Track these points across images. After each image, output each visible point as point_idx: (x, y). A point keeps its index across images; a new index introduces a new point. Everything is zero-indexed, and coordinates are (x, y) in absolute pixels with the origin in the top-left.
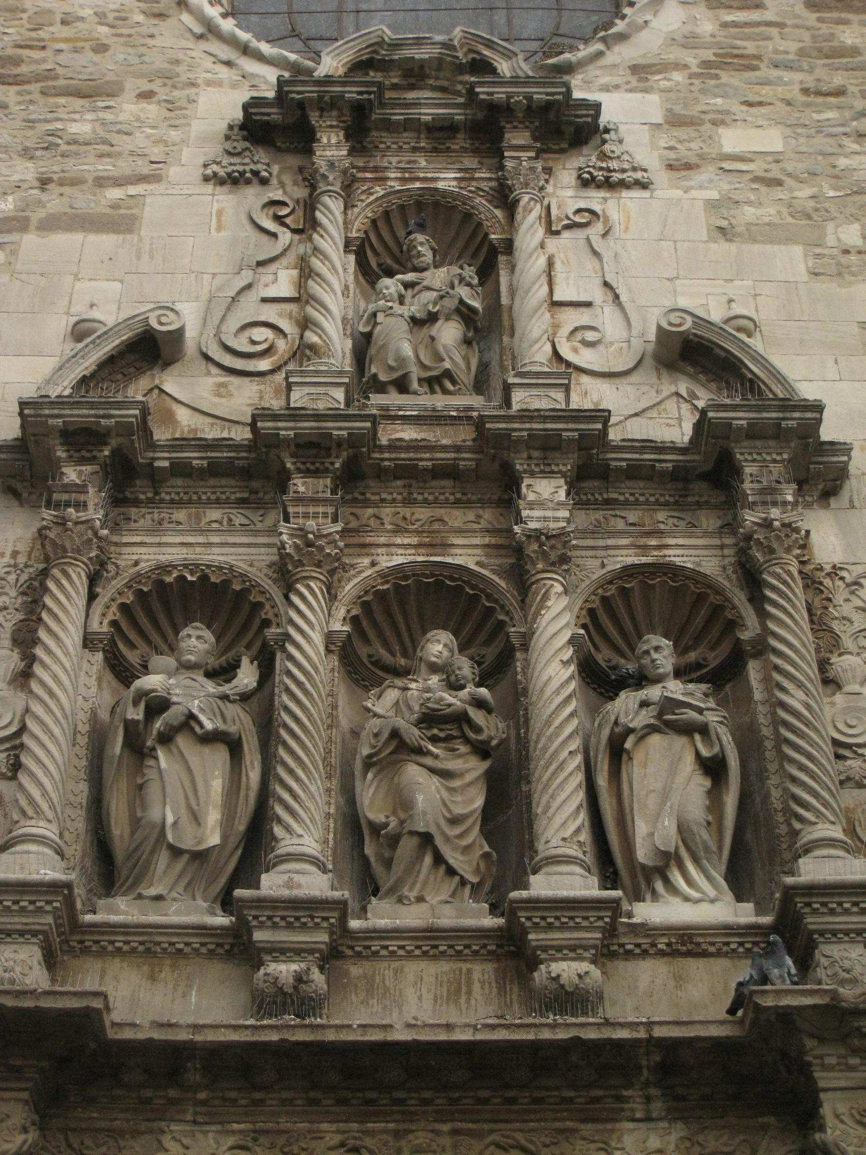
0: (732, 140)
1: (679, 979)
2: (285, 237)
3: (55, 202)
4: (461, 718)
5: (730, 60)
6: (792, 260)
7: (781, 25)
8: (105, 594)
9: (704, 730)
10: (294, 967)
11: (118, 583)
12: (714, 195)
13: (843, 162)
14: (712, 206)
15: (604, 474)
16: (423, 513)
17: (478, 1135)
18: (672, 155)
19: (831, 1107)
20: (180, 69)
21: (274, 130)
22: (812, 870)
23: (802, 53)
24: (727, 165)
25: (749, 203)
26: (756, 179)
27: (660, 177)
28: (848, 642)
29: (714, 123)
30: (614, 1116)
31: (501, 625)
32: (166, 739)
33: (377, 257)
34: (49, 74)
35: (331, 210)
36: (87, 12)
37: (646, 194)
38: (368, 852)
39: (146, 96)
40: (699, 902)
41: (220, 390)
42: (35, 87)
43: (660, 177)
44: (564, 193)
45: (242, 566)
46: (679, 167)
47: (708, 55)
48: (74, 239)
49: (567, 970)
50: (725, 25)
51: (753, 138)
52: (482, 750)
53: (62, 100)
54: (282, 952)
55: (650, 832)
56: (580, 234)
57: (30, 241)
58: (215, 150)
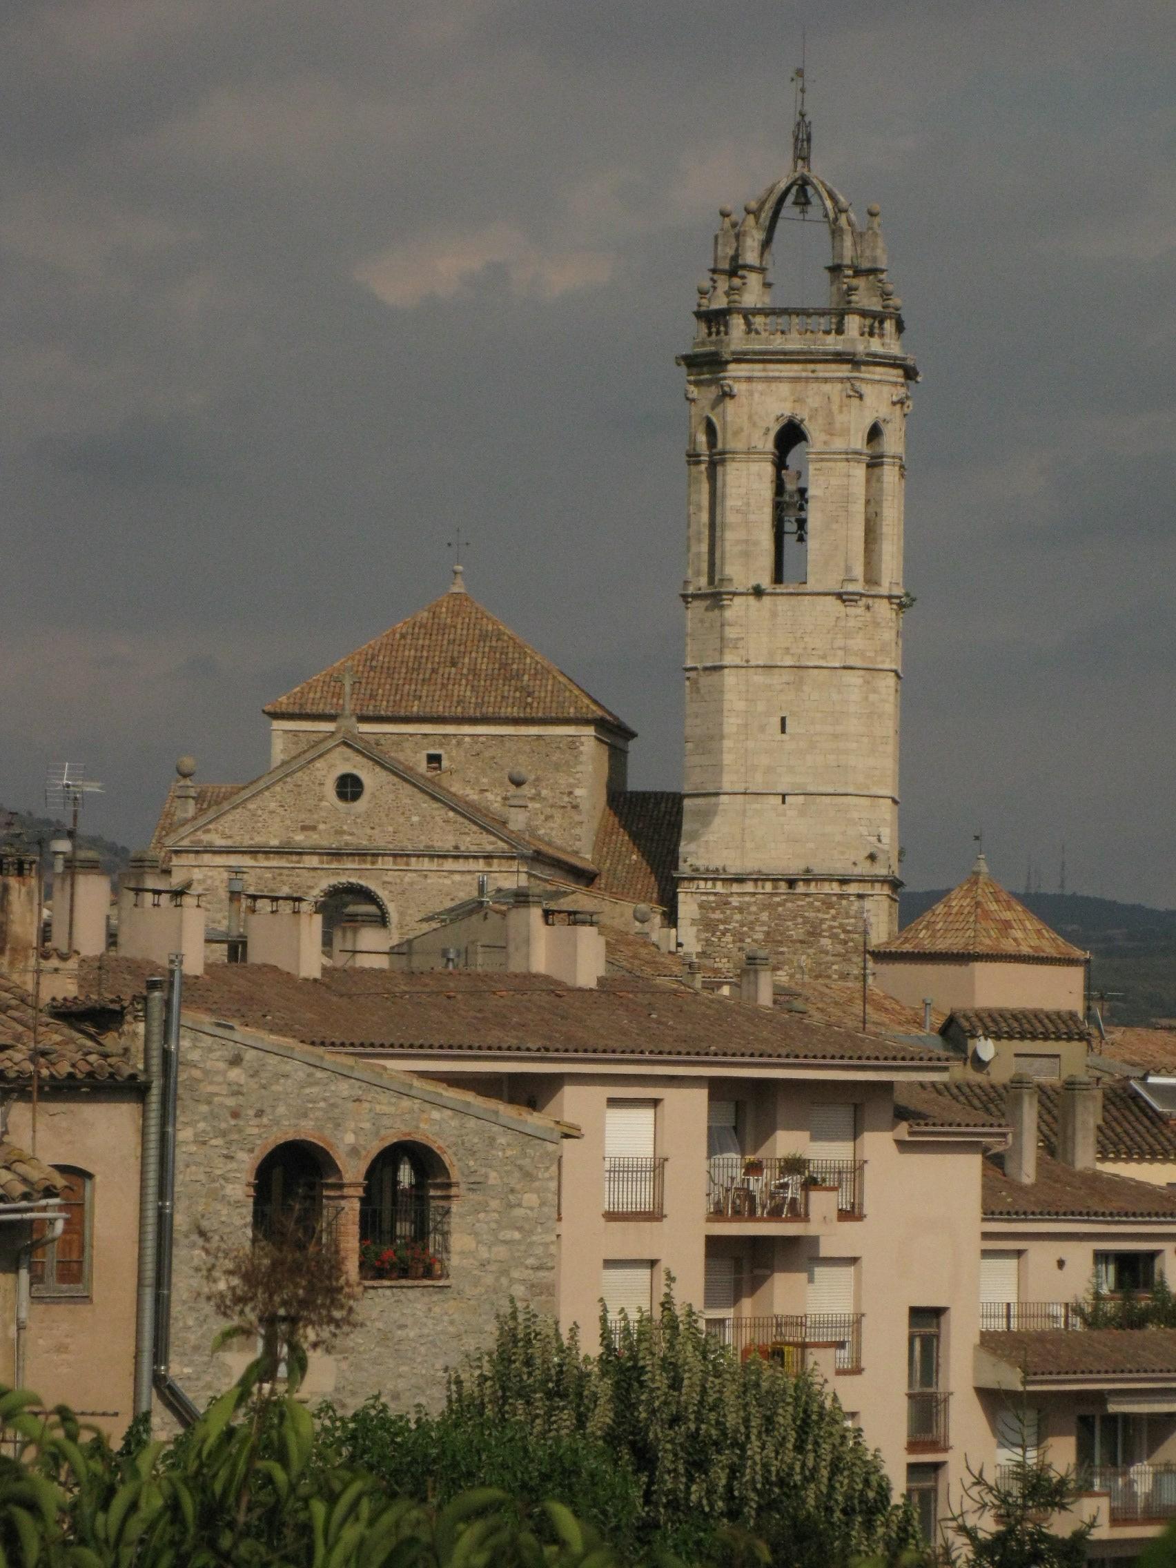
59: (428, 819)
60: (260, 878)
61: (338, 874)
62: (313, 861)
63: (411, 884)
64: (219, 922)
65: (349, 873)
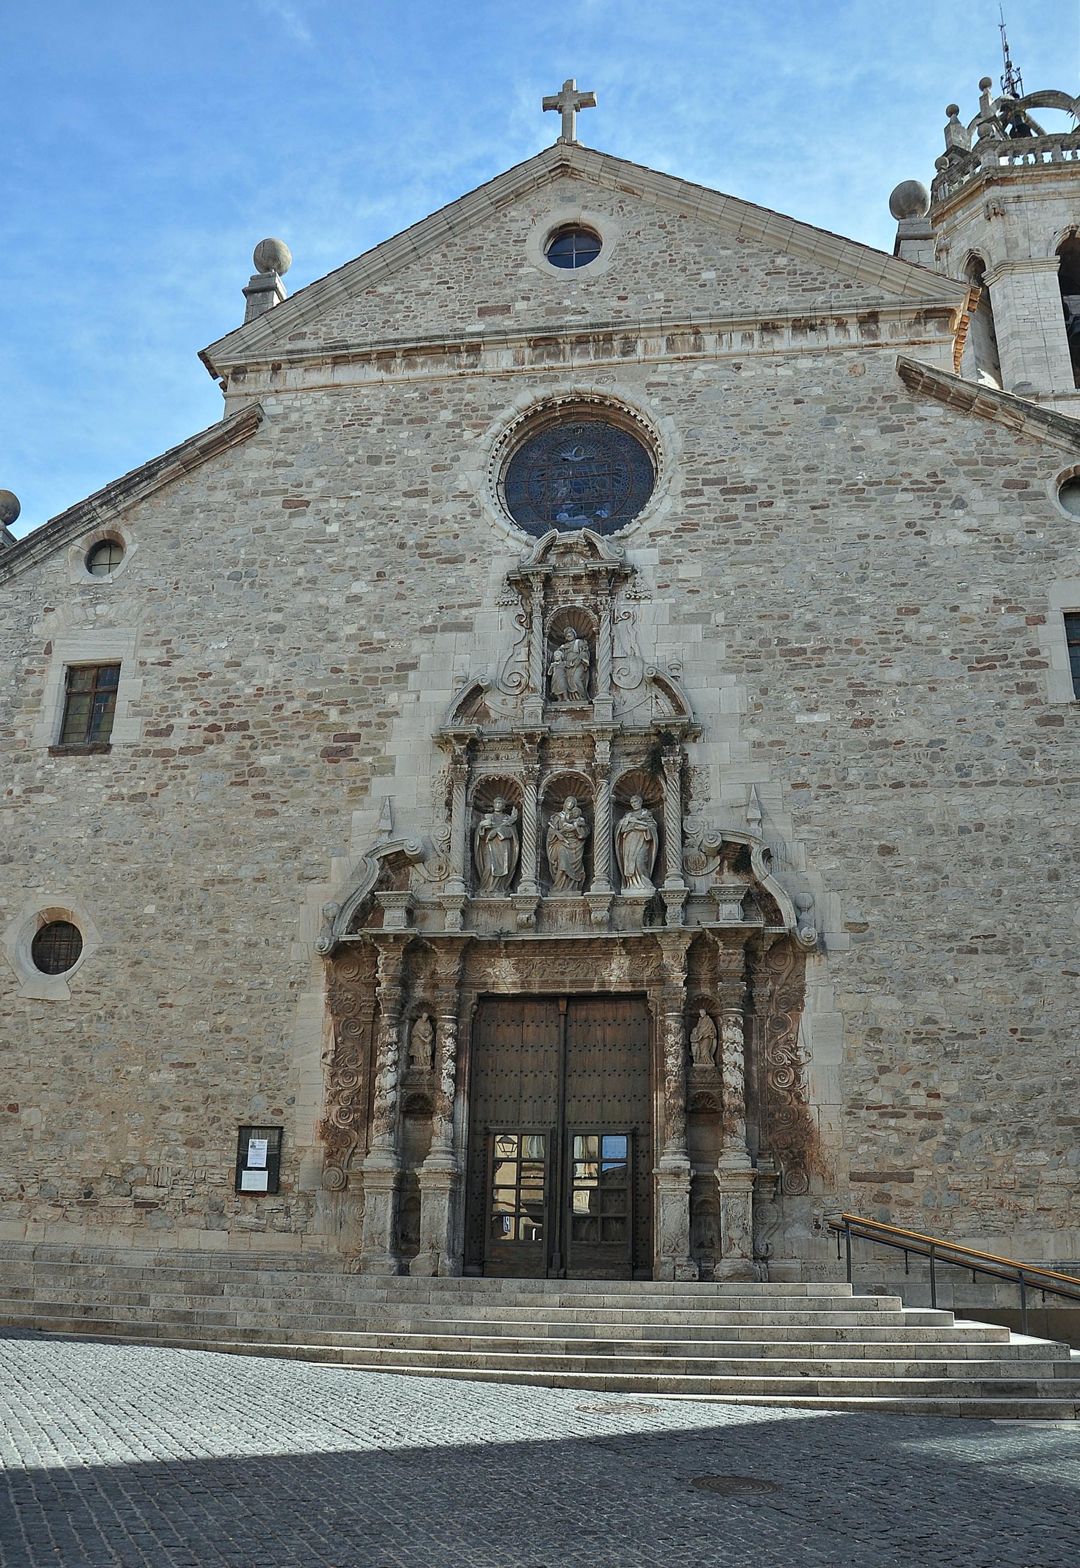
0: (683, 571)
6: (696, 631)
7: (709, 505)
11: (475, 783)
12: (673, 601)
13: (723, 580)
14: (672, 606)
18: (660, 580)
20: (485, 546)
21: (519, 582)
24: (679, 584)
25: (686, 603)
27: (655, 592)
33: (555, 639)
37: (649, 602)
39: (475, 561)
45: (512, 776)
47: (679, 524)
51: (690, 570)
53: (444, 566)
55: (629, 868)
57: (438, 635)
58: (498, 589)
59: (736, 272)
64: (310, 484)
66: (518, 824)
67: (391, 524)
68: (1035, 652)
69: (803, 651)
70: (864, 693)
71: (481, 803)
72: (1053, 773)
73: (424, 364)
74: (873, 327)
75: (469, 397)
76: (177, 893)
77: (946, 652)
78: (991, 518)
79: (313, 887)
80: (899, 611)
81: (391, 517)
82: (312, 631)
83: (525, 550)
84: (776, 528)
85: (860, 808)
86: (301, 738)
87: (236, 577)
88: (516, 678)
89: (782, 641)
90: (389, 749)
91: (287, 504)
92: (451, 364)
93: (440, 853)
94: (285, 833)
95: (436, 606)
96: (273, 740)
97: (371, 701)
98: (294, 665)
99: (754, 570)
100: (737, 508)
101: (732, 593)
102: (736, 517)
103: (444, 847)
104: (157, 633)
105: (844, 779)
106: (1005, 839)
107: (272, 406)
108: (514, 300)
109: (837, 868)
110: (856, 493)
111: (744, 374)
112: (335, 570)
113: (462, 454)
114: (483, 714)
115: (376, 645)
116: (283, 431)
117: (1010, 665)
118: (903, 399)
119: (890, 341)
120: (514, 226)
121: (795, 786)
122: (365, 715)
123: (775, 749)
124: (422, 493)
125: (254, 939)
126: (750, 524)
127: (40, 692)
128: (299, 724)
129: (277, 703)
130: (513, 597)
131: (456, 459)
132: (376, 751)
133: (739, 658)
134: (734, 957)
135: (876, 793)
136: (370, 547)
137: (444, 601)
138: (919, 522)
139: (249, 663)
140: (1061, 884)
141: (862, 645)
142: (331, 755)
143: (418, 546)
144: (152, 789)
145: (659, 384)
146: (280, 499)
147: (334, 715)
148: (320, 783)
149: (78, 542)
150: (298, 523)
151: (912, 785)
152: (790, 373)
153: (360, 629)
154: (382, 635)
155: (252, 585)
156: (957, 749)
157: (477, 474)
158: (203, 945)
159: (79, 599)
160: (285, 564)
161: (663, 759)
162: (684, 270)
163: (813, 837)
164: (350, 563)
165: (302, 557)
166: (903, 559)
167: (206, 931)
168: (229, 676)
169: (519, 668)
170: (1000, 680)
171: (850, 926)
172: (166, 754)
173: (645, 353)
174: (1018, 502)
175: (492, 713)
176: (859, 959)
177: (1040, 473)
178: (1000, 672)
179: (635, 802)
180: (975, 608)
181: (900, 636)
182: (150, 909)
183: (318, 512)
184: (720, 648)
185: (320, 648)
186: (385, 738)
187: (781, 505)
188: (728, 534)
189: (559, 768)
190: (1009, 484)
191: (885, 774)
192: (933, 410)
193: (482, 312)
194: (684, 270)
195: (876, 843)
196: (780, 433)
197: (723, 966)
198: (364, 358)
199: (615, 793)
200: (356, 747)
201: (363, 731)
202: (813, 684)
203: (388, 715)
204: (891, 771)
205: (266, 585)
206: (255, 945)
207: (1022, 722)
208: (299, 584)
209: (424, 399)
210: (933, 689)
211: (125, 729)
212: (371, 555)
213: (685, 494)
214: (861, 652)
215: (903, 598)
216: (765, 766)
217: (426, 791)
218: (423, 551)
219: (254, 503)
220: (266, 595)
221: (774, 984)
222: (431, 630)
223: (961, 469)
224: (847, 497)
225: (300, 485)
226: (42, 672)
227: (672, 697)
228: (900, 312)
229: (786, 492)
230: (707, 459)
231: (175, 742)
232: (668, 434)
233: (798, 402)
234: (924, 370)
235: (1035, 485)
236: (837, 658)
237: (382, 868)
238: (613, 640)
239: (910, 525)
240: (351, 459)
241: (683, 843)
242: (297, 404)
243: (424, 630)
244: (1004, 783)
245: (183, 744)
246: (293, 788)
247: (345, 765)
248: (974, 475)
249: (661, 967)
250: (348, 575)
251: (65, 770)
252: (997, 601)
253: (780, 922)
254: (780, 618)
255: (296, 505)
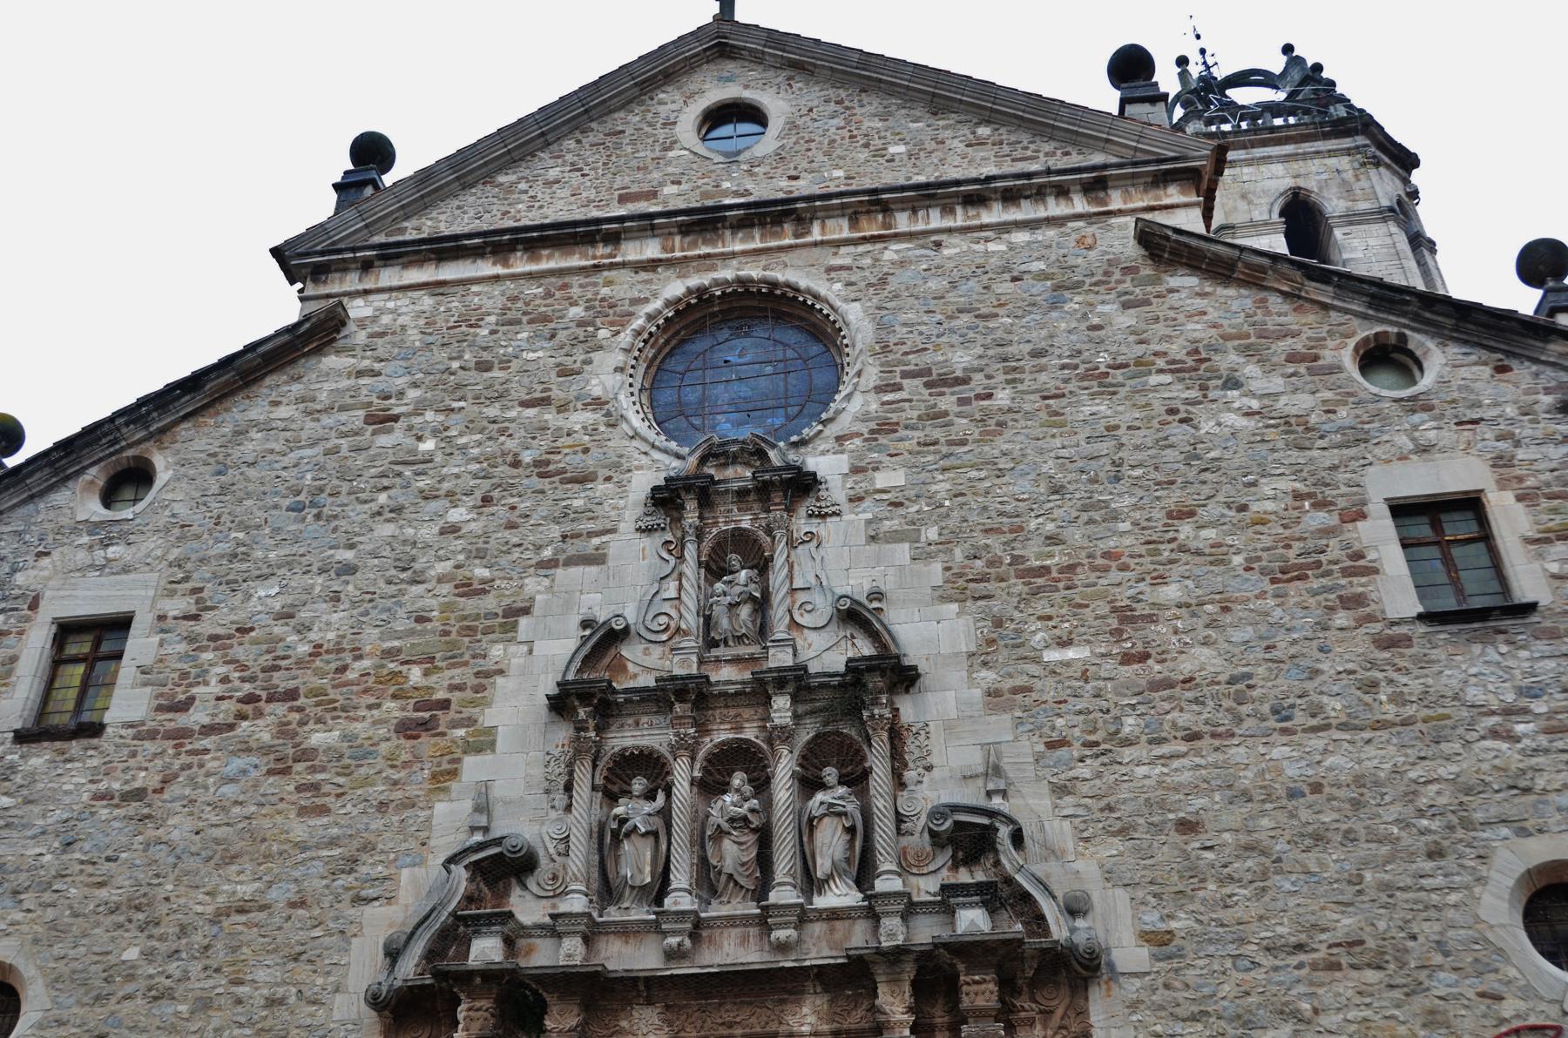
0: (882, 480)
1: (832, 930)
2: (673, 561)
3: (572, 548)
4: (745, 819)
5: (886, 427)
6: (903, 551)
7: (910, 401)
8: (601, 764)
9: (845, 814)
10: (678, 939)
12: (869, 516)
13: (934, 488)
14: (869, 522)
15: (809, 688)
16: (732, 712)
17: (750, 1003)
18: (852, 492)
19: (882, 989)
20: (623, 461)
21: (666, 499)
22: (881, 885)
23: (920, 418)
26: (892, 504)
27: (845, 507)
28: (911, 765)
29: (876, 469)
30: (803, 992)
31: (766, 767)
32: (627, 835)
33: (715, 569)
34: (563, 471)
35: (690, 551)
36: (577, 427)
38: (708, 881)
39: (608, 479)
40: (842, 895)
41: (646, 652)
42: (557, 479)
43: (845, 507)
44: (801, 524)
45: (657, 746)
46: (856, 499)
47: (873, 425)
48: (581, 568)
49: (781, 934)
50: (883, 404)
51: (890, 478)
52: (754, 831)
54: (674, 933)
55: (823, 866)
56: (806, 546)
57: (560, 572)
58: (640, 511)
60: (514, 299)
61: (713, 268)
62: (651, 249)
63: (902, 264)
64: (401, 394)
65: (739, 261)
66: (665, 814)
67: (503, 438)
68: (1359, 556)
69: (1045, 570)
70: (1132, 620)
71: (615, 789)
72: (1410, 710)
73: (549, 257)
74: (1102, 194)
75: (605, 291)
76: (173, 930)
77: (1238, 560)
78: (1275, 396)
79: (369, 910)
80: (1170, 515)
81: (502, 432)
82: (393, 572)
83: (676, 463)
84: (999, 424)
85: (1142, 770)
86: (370, 707)
87: (297, 508)
88: (663, 619)
89: (1016, 560)
90: (488, 718)
91: (370, 420)
92: (584, 256)
93: (555, 857)
94: (338, 838)
95: (557, 534)
96: (333, 709)
97: (467, 657)
98: (366, 613)
99: (974, 474)
100: (947, 402)
101: (947, 503)
102: (946, 414)
103: (561, 847)
104: (186, 579)
105: (1117, 732)
106: (1357, 804)
107: (357, 309)
108: (662, 184)
109: (1121, 854)
110: (1100, 381)
111: (946, 252)
112: (427, 496)
113: (596, 356)
114: (620, 666)
115: (476, 586)
116: (371, 336)
117: (1328, 574)
118: (1147, 271)
119: (1123, 207)
120: (661, 108)
121: (1051, 745)
122: (457, 675)
123: (1019, 697)
124: (544, 402)
125: (280, 991)
126: (965, 421)
127: (14, 659)
128: (366, 691)
129: (339, 663)
130: (660, 519)
131: (589, 362)
132: (470, 722)
133: (961, 582)
134: (984, 986)
135: (1165, 749)
136: (474, 467)
137: (568, 528)
138: (1182, 408)
139: (304, 615)
140: (1449, 862)
141: (1124, 559)
142: (408, 729)
143: (537, 463)
144: (154, 781)
145: (841, 268)
146: (361, 413)
147: (415, 674)
148: (393, 767)
149: (93, 471)
150: (384, 440)
151: (1214, 735)
152: (1003, 247)
153: (458, 567)
154: (486, 573)
155: (318, 517)
156: (1270, 686)
157: (610, 373)
158: (204, 1004)
159: (85, 539)
160: (364, 491)
161: (865, 714)
162: (866, 145)
163: (1080, 811)
164: (446, 486)
165: (386, 482)
166: (1168, 451)
167: (211, 982)
168: (278, 630)
169: (667, 607)
170: (1315, 594)
171: (1148, 937)
172: (181, 735)
173: (823, 233)
174: (1309, 378)
175: (630, 666)
176: (1167, 986)
177: (1330, 344)
178: (1315, 584)
179: (830, 774)
180: (1270, 506)
181: (1174, 545)
182: (132, 954)
183: (410, 428)
184: (935, 572)
185: (402, 592)
186: (486, 703)
187: (1003, 397)
188: (937, 434)
189: (722, 735)
190: (1292, 358)
191: (1174, 725)
192: (1185, 281)
193: (623, 199)
194: (866, 145)
195: (1171, 816)
196: (996, 315)
197: (966, 1002)
198: (476, 253)
199: (800, 765)
200: (444, 718)
201: (455, 697)
202: (1064, 611)
203: (488, 675)
204: (1184, 719)
205: (335, 517)
206: (281, 1002)
207: (1352, 648)
208: (379, 514)
209: (549, 295)
210: (1226, 609)
211: (127, 703)
212: (475, 476)
213: (879, 389)
214: (1124, 568)
215: (1173, 497)
216: (1006, 718)
217: (538, 772)
218: (542, 467)
219: (327, 420)
220: (335, 530)
221: (1045, 1027)
222: (552, 563)
223: (1230, 344)
224: (1086, 384)
225: (388, 398)
226: (21, 633)
227: (874, 636)
228: (1134, 176)
229: (1008, 382)
230: (905, 348)
231: (197, 717)
232: (856, 318)
233: (1015, 279)
234: (1170, 233)
235: (1328, 356)
236: (1093, 577)
237: (471, 880)
238: (791, 567)
239: (1172, 411)
240: (455, 365)
241: (898, 829)
242: (391, 305)
243: (542, 565)
244: (1343, 727)
245: (206, 720)
246: (355, 775)
247: (426, 743)
248: (1248, 351)
249: (874, 1009)
250: (445, 502)
251: (35, 762)
252: (1298, 496)
253: (1046, 931)
254: (1011, 531)
255: (382, 420)
